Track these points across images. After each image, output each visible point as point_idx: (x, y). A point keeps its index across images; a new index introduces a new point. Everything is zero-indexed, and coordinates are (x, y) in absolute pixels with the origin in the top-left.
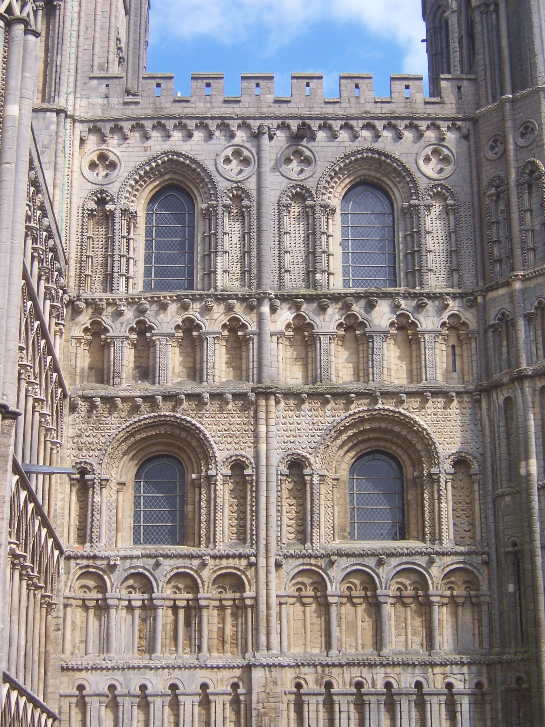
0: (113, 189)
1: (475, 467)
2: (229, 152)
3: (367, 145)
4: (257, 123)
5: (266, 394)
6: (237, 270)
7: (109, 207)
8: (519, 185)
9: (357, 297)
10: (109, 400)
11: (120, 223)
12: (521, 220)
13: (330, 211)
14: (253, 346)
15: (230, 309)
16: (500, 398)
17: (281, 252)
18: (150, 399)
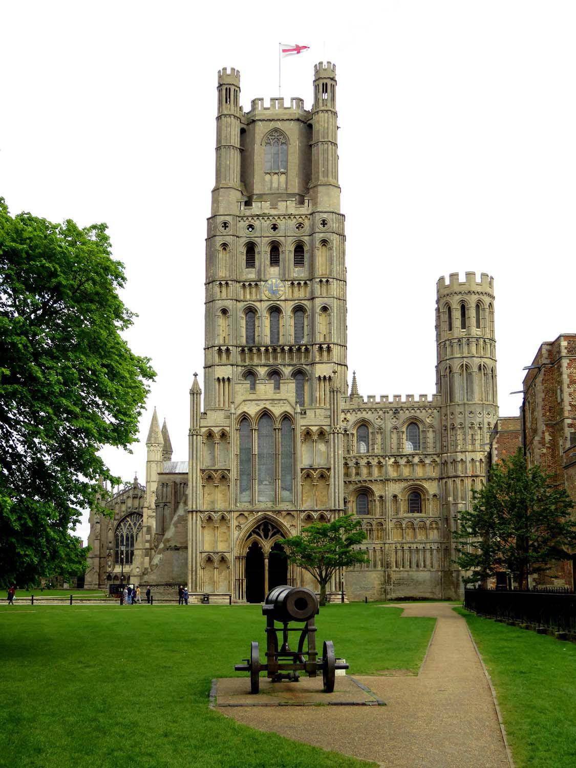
0: (348, 427)
1: (438, 497)
2: (377, 417)
3: (412, 415)
4: (384, 410)
5: (388, 480)
6: (380, 448)
7: (348, 432)
8: (450, 429)
9: (410, 455)
10: (350, 482)
11: (350, 436)
12: (451, 438)
13: (403, 432)
14: (384, 468)
15: (379, 459)
16: (444, 481)
17: (391, 444)
18: (360, 481)
